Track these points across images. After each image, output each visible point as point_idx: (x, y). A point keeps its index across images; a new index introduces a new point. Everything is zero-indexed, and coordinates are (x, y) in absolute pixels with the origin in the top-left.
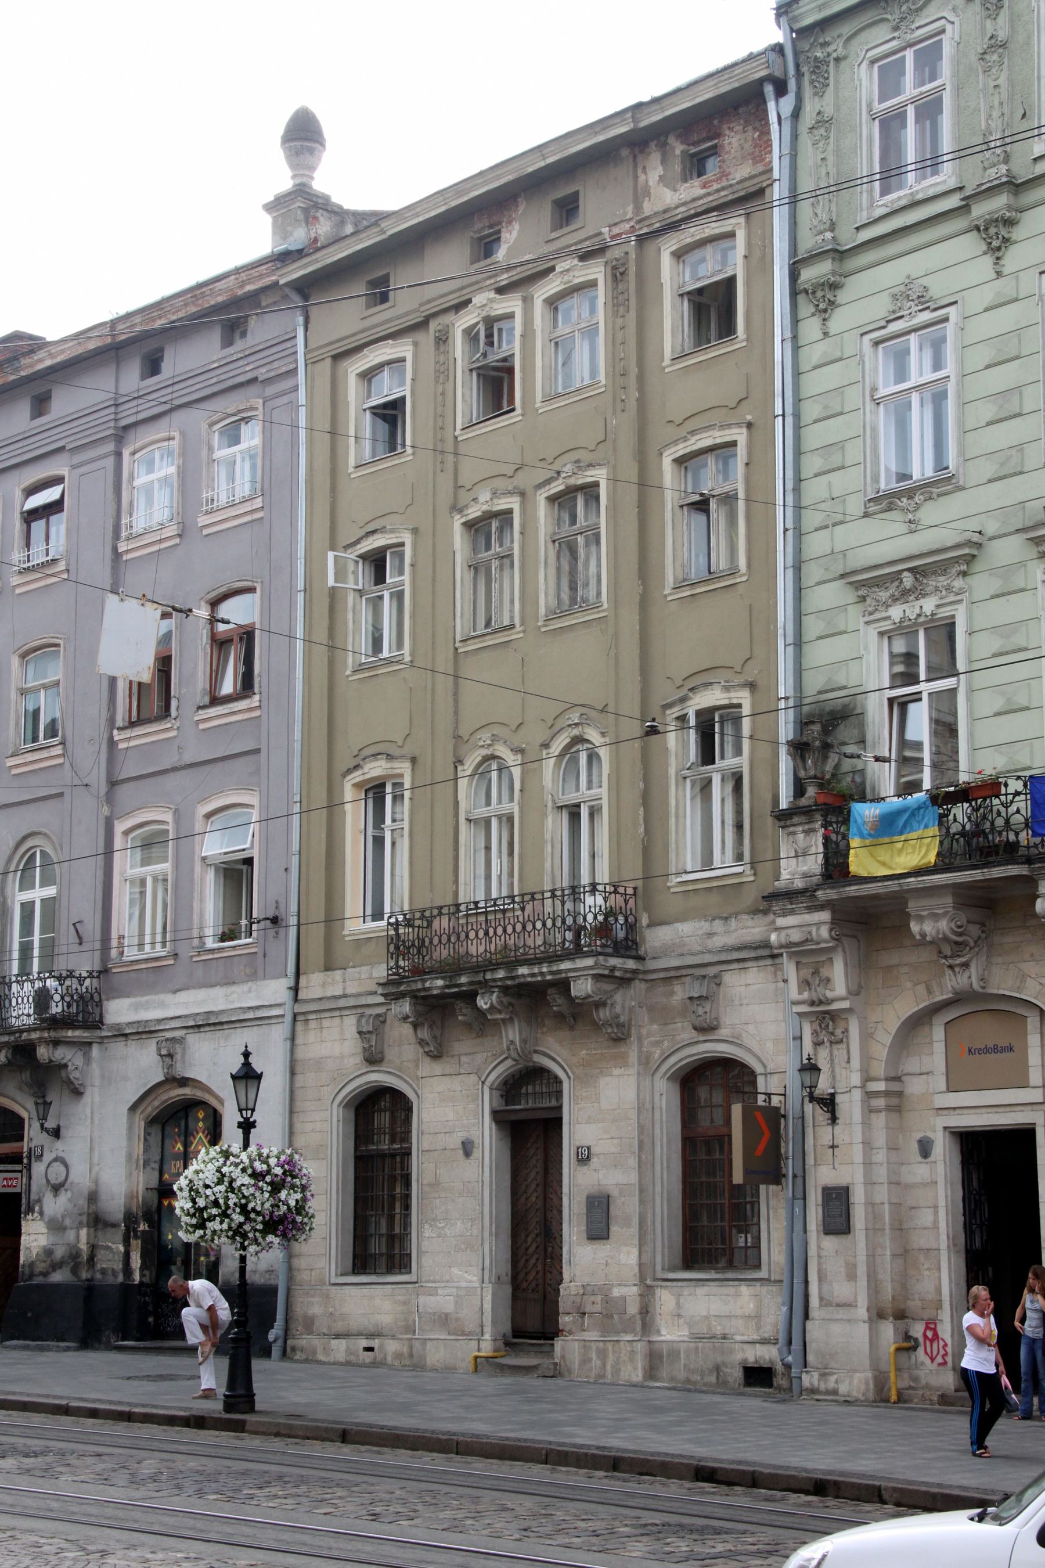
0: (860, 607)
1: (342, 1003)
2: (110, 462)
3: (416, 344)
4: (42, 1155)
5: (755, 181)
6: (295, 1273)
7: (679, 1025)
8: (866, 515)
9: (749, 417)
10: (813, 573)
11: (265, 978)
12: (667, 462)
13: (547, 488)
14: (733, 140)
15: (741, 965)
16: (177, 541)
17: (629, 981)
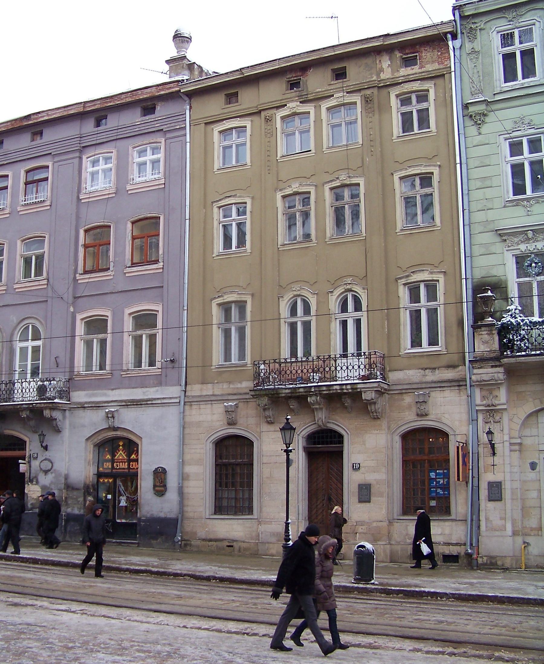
0: (503, 244)
1: (213, 398)
2: (76, 161)
3: (252, 121)
4: (37, 457)
5: (441, 71)
6: (185, 513)
7: (407, 413)
8: (505, 207)
9: (439, 163)
10: (477, 229)
11: (166, 385)
12: (396, 177)
13: (330, 184)
14: (428, 54)
15: (441, 389)
16: (114, 195)
17: (384, 393)
